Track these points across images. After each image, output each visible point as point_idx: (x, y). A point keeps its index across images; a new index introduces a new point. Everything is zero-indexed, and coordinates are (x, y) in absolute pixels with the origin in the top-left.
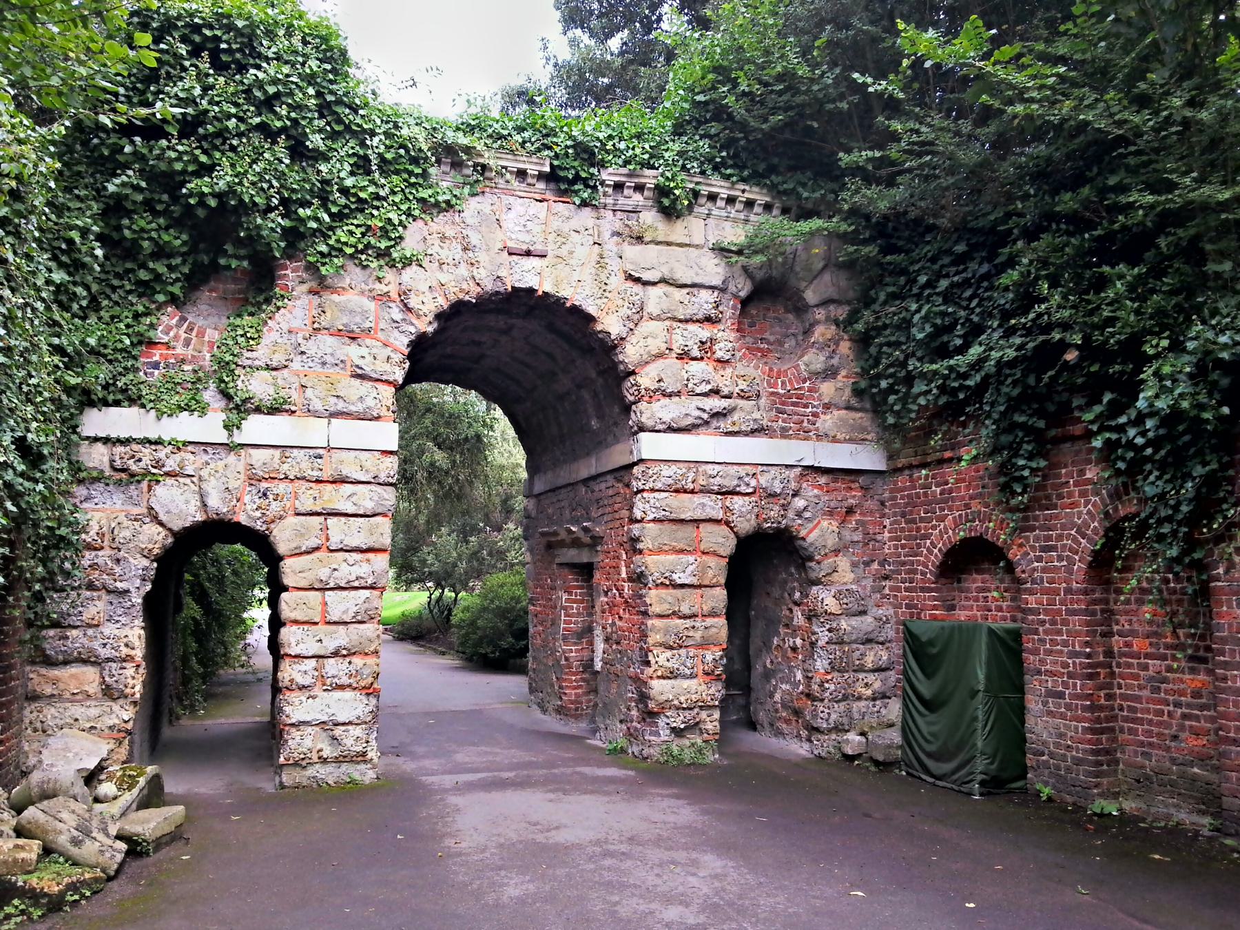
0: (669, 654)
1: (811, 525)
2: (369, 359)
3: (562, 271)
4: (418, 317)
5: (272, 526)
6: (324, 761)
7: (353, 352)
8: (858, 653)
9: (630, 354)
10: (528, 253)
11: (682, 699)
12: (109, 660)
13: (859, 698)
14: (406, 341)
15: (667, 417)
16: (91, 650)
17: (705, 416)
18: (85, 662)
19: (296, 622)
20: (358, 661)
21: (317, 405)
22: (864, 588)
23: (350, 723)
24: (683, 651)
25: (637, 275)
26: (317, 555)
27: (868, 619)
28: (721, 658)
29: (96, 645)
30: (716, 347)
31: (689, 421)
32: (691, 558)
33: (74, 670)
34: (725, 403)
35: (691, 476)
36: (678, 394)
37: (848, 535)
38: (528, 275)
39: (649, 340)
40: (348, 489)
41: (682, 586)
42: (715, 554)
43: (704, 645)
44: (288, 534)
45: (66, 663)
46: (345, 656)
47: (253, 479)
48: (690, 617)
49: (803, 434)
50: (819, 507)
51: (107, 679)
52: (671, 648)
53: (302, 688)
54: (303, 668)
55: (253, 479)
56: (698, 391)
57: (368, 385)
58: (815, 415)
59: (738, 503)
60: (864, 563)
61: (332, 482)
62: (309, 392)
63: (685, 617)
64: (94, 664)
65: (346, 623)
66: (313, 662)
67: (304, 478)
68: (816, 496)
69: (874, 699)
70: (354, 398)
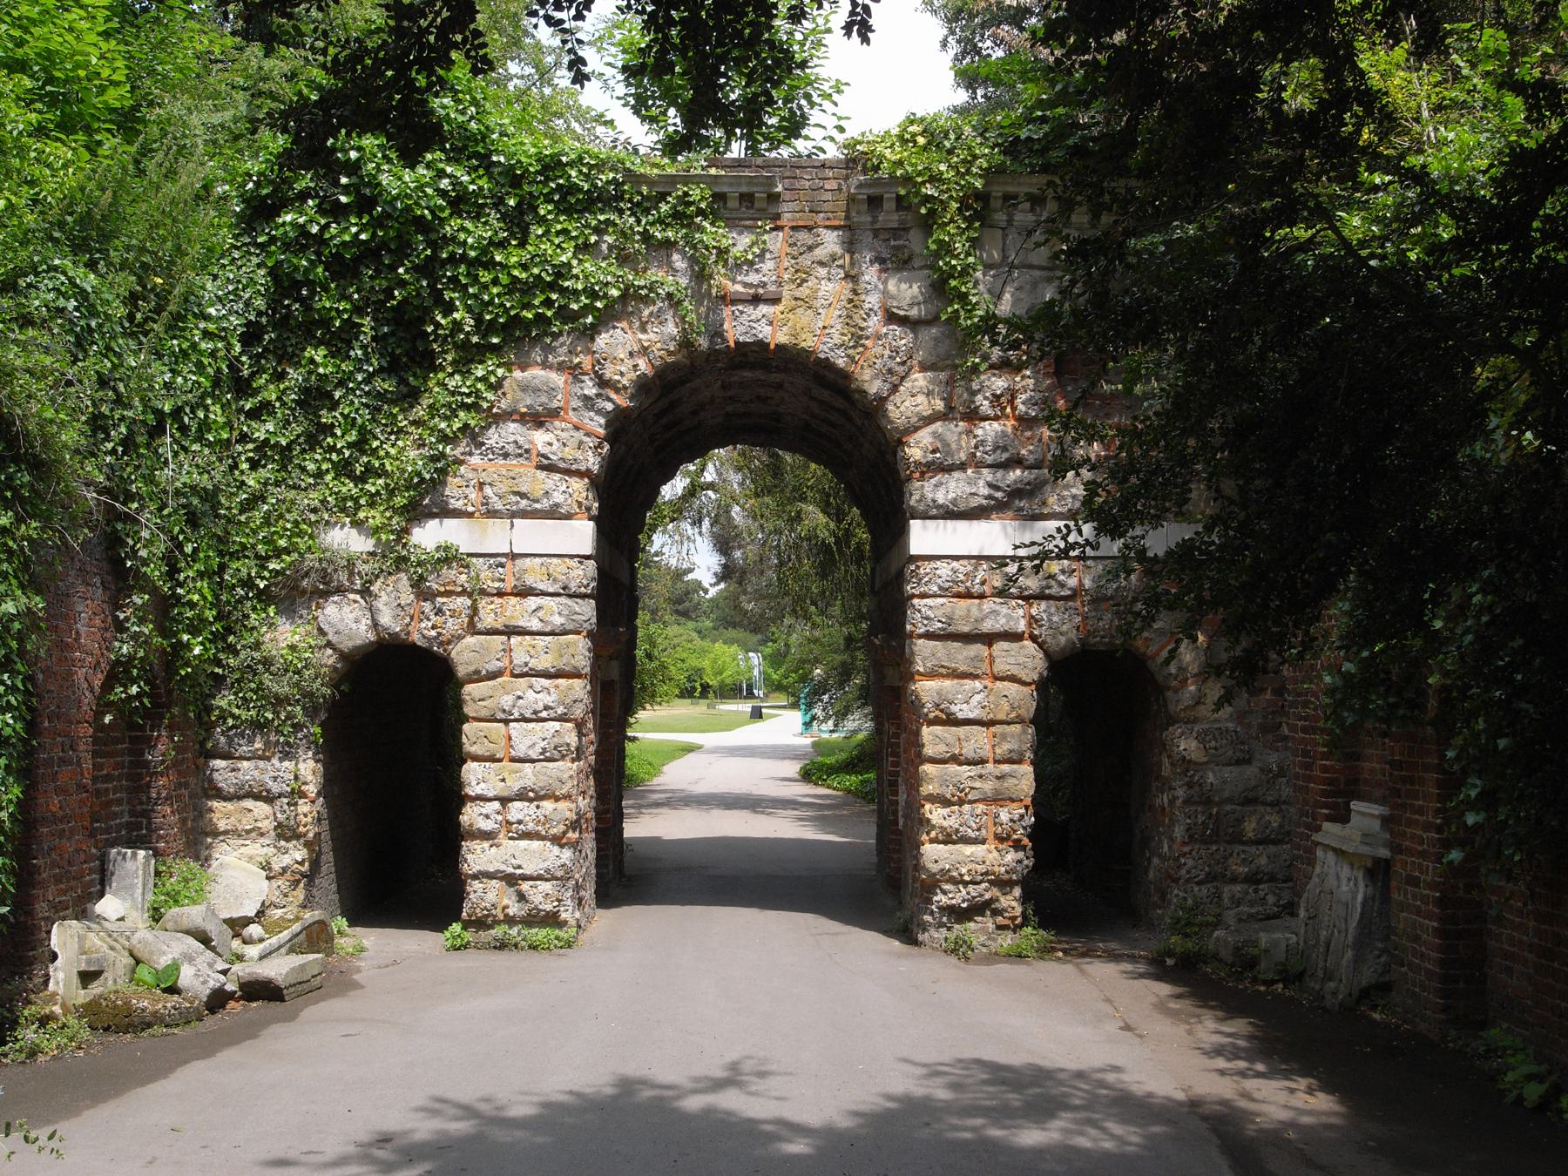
0: (945, 811)
2: (556, 445)
3: (803, 317)
4: (617, 391)
6: (510, 921)
7: (540, 439)
11: (964, 871)
13: (1234, 880)
18: (257, 797)
19: (476, 758)
20: (548, 806)
23: (539, 878)
24: (966, 807)
27: (1251, 771)
31: (975, 502)
32: (978, 684)
40: (533, 602)
42: (1013, 679)
43: (997, 799)
46: (531, 800)
51: (279, 815)
53: (487, 836)
57: (557, 476)
61: (516, 595)
62: (488, 490)
63: (969, 763)
65: (533, 761)
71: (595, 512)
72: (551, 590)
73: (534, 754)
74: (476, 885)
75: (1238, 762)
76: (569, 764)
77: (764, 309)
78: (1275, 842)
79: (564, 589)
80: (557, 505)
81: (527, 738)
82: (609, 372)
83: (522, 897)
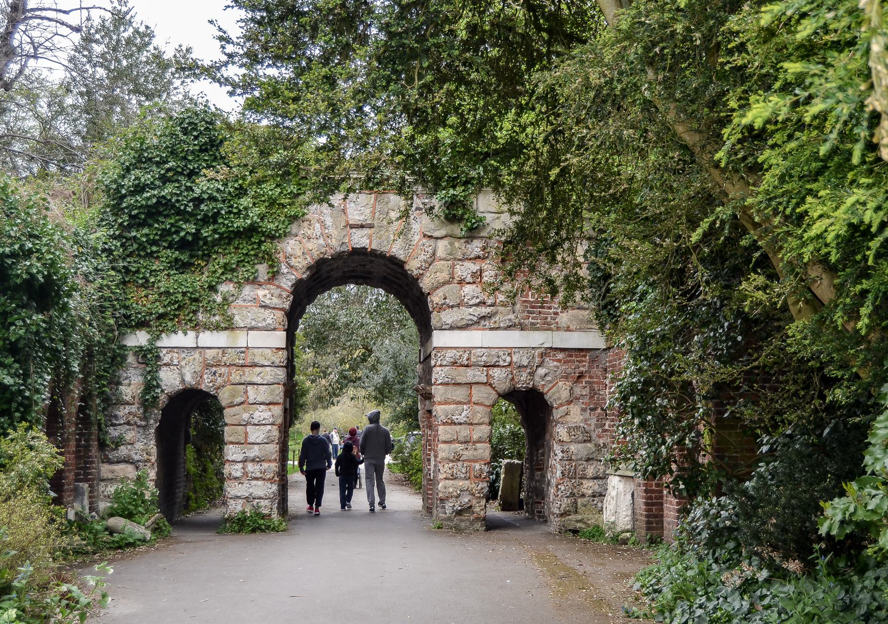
2: (269, 296)
4: (297, 270)
9: (425, 284)
10: (362, 226)
12: (138, 461)
14: (290, 284)
15: (449, 321)
16: (129, 456)
17: (475, 319)
19: (232, 443)
20: (265, 465)
22: (590, 425)
24: (459, 464)
25: (429, 234)
26: (242, 406)
29: (132, 453)
30: (484, 275)
31: (464, 322)
33: (122, 466)
34: (489, 310)
35: (466, 356)
36: (458, 306)
37: (578, 391)
38: (360, 240)
39: (438, 274)
40: (258, 369)
41: (460, 424)
44: (226, 395)
45: (118, 462)
48: (465, 442)
49: (547, 327)
52: (452, 461)
53: (236, 478)
55: (208, 366)
56: (471, 303)
57: (268, 311)
58: (556, 314)
59: (496, 373)
60: (590, 409)
63: (462, 443)
64: (132, 463)
65: (258, 444)
66: (240, 465)
67: (234, 365)
68: (555, 366)
69: (594, 496)
70: (260, 319)
71: (286, 327)
73: (258, 441)
74: (232, 502)
75: (585, 441)
77: (366, 231)
78: (601, 478)
82: (293, 262)
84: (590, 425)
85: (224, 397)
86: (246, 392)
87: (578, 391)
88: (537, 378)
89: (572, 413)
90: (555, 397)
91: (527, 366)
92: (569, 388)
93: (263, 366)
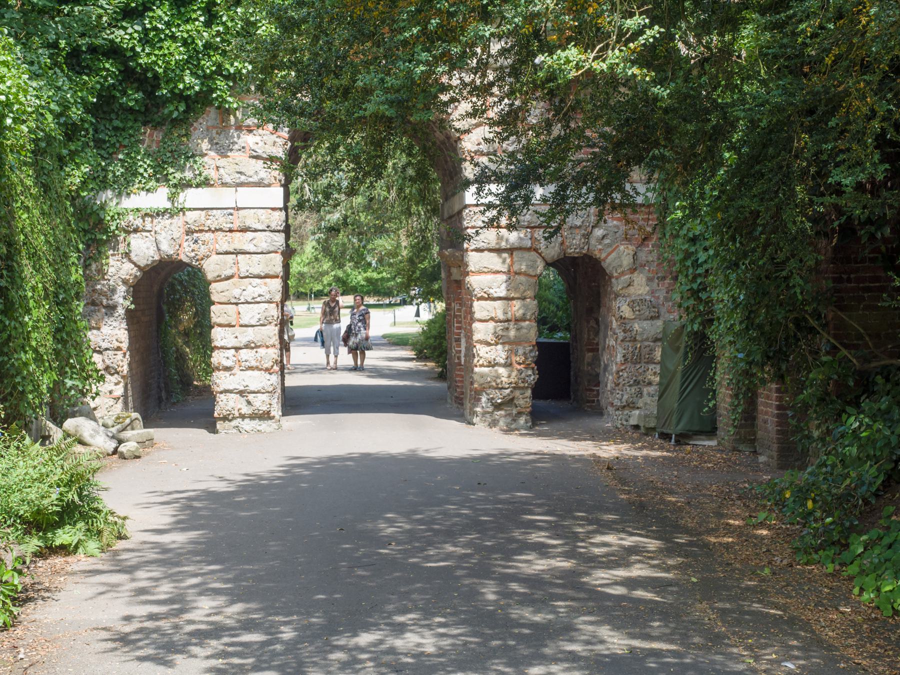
0: (488, 349)
1: (610, 249)
2: (261, 144)
5: (202, 262)
6: (243, 417)
8: (648, 349)
12: (106, 349)
19: (220, 325)
20: (262, 351)
21: (227, 179)
22: (658, 298)
23: (258, 392)
28: (531, 351)
37: (643, 256)
40: (250, 235)
46: (252, 348)
47: (189, 232)
50: (618, 235)
51: (106, 361)
53: (227, 369)
54: (226, 355)
61: (240, 231)
62: (221, 170)
63: (501, 322)
65: (253, 326)
67: (221, 230)
68: (615, 226)
71: (283, 182)
72: (260, 228)
73: (253, 322)
74: (222, 396)
75: (652, 318)
76: (274, 327)
79: (268, 227)
80: (262, 179)
81: (250, 314)
83: (249, 403)
84: (658, 298)
85: (211, 268)
86: (236, 263)
87: (643, 256)
88: (593, 241)
89: (636, 282)
90: (614, 264)
91: (580, 227)
92: (632, 253)
93: (256, 231)
